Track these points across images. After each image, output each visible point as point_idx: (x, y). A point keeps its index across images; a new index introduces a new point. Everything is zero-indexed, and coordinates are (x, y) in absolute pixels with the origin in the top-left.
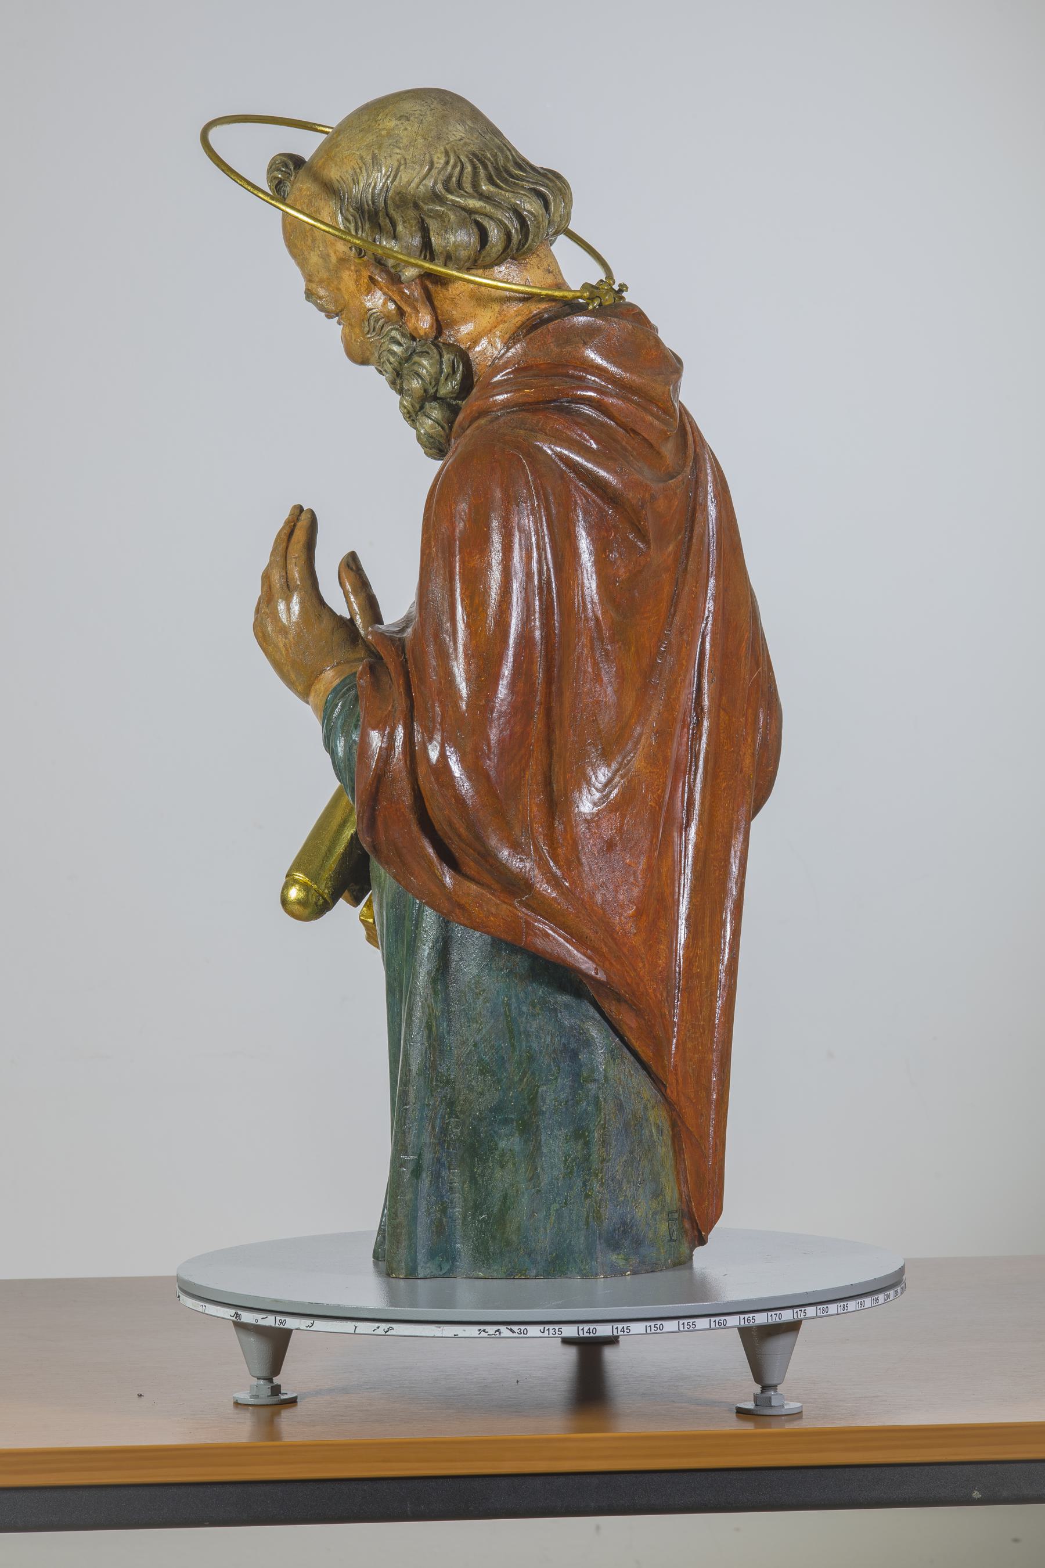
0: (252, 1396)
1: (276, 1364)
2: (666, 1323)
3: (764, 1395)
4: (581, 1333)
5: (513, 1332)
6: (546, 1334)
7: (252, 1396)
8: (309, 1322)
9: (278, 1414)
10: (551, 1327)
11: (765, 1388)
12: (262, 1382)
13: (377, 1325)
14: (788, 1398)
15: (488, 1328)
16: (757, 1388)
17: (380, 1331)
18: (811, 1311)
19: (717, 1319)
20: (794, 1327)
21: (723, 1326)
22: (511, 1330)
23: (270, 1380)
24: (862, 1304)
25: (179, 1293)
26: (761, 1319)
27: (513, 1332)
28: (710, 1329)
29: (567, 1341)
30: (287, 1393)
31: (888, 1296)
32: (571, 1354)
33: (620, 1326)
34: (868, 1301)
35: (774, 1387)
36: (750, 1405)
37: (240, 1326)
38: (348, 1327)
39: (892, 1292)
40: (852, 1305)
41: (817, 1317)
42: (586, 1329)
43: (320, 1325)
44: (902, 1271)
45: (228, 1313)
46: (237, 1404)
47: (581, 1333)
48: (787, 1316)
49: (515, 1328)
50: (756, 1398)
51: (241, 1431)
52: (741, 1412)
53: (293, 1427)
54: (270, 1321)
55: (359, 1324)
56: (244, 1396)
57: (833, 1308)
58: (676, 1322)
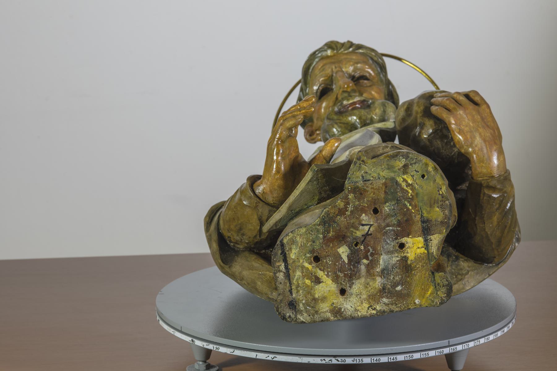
4: (372, 361)
5: (339, 361)
6: (355, 362)
8: (232, 350)
12: (201, 363)
13: (267, 355)
15: (326, 359)
19: (439, 350)
22: (337, 360)
27: (339, 361)
42: (375, 359)
45: (188, 339)
47: (372, 361)
49: (339, 359)
54: (211, 347)
55: (257, 354)
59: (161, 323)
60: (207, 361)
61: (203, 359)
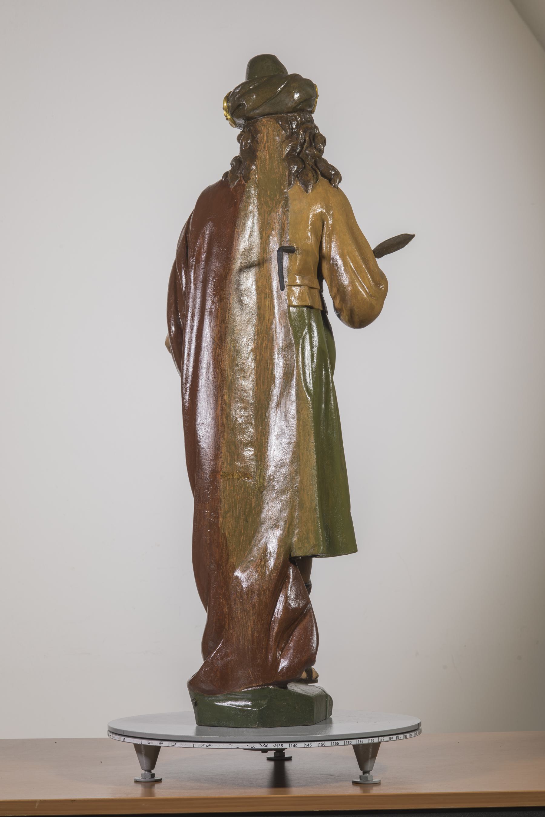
0: (143, 778)
1: (153, 765)
2: (326, 742)
3: (365, 775)
7: (143, 778)
8: (173, 743)
9: (154, 785)
10: (278, 744)
11: (365, 773)
12: (147, 772)
14: (375, 775)
16: (361, 773)
17: (205, 746)
18: (386, 738)
20: (377, 745)
21: (349, 744)
23: (150, 771)
24: (406, 736)
25: (110, 734)
26: (365, 741)
28: (345, 745)
29: (269, 759)
30: (157, 777)
31: (416, 734)
32: (271, 764)
33: (307, 743)
34: (408, 735)
35: (368, 772)
36: (359, 780)
37: (138, 747)
38: (191, 744)
39: (417, 732)
40: (402, 736)
41: (388, 741)
43: (178, 744)
44: (420, 723)
46: (136, 782)
48: (376, 740)
50: (360, 777)
51: (137, 792)
52: (354, 783)
53: (160, 792)
55: (195, 743)
56: (139, 778)
57: (394, 737)
58: (330, 742)
59: (112, 735)
60: (153, 771)
61: (148, 769)
